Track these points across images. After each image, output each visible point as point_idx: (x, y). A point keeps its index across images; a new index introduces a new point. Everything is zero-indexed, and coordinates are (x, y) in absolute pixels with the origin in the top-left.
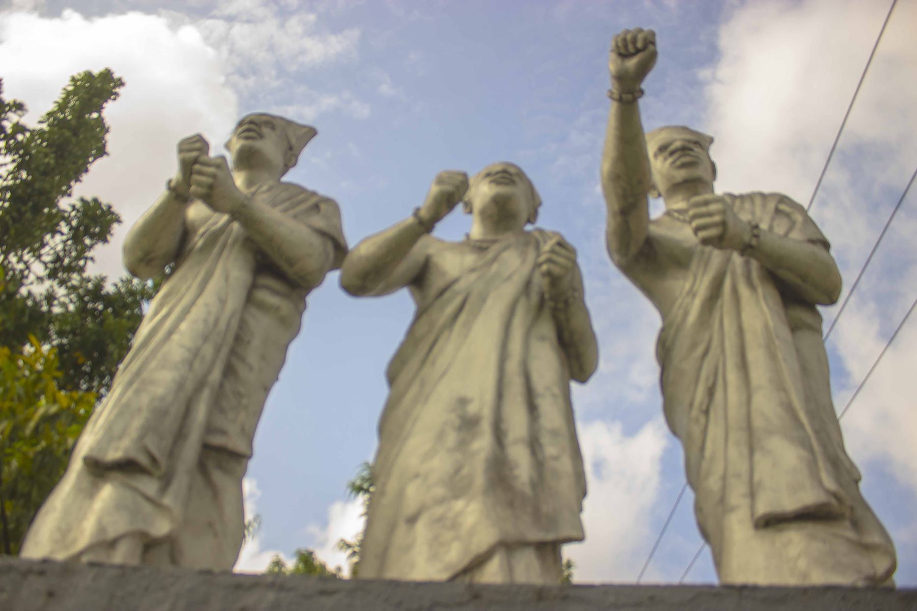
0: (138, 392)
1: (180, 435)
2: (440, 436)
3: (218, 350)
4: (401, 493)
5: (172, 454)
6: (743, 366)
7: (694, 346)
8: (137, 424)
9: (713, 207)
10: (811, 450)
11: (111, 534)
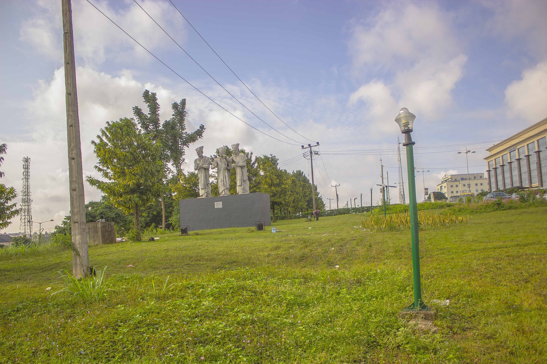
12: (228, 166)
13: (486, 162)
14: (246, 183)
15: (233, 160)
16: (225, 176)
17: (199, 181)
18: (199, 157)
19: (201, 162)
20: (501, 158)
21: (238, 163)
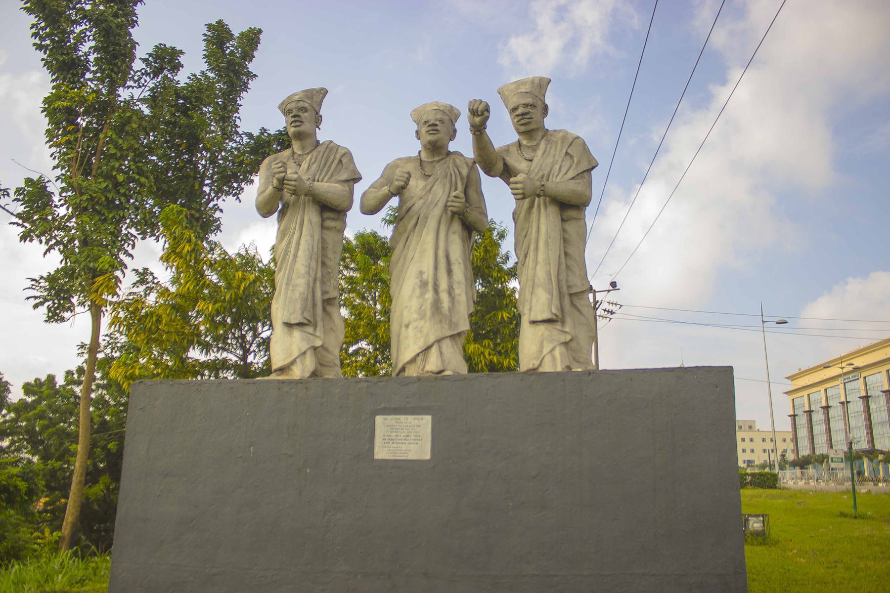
0: (293, 291)
1: (314, 305)
2: (414, 290)
3: (317, 262)
4: (402, 314)
5: (314, 315)
6: (537, 249)
7: (522, 229)
8: (298, 306)
9: (519, 186)
10: (552, 296)
11: (303, 351)
13: (788, 399)
14: (579, 311)
16: (447, 257)
19: (305, 165)
20: (823, 392)
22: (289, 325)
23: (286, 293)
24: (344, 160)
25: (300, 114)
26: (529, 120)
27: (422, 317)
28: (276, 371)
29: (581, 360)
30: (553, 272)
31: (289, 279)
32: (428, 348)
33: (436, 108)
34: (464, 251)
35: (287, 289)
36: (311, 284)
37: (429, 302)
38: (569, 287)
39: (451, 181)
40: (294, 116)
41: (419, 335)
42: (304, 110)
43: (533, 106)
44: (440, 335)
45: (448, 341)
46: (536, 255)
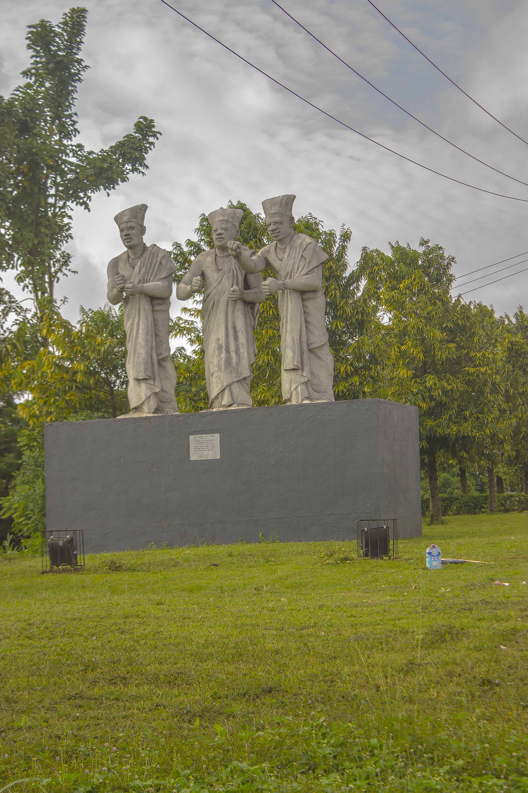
0: (138, 357)
1: (153, 365)
3: (152, 336)
5: (153, 372)
6: (286, 322)
8: (142, 367)
9: (266, 287)
12: (247, 286)
14: (319, 358)
15: (268, 264)
16: (234, 328)
17: (129, 346)
18: (130, 247)
19: (137, 269)
21: (290, 274)
22: (138, 380)
23: (134, 359)
24: (163, 262)
25: (130, 232)
26: (277, 234)
27: (220, 370)
28: (133, 409)
29: (321, 390)
30: (296, 337)
31: (135, 349)
32: (223, 390)
33: (222, 218)
34: (246, 323)
35: (134, 356)
36: (149, 352)
37: (223, 359)
38: (308, 345)
39: (233, 276)
40: (126, 235)
41: (219, 381)
42: (132, 228)
43: (280, 223)
44: (230, 381)
45: (236, 384)
46: (286, 326)
